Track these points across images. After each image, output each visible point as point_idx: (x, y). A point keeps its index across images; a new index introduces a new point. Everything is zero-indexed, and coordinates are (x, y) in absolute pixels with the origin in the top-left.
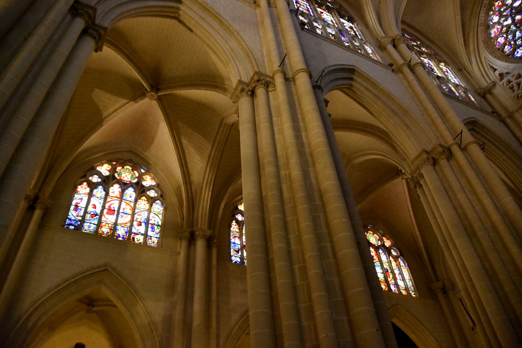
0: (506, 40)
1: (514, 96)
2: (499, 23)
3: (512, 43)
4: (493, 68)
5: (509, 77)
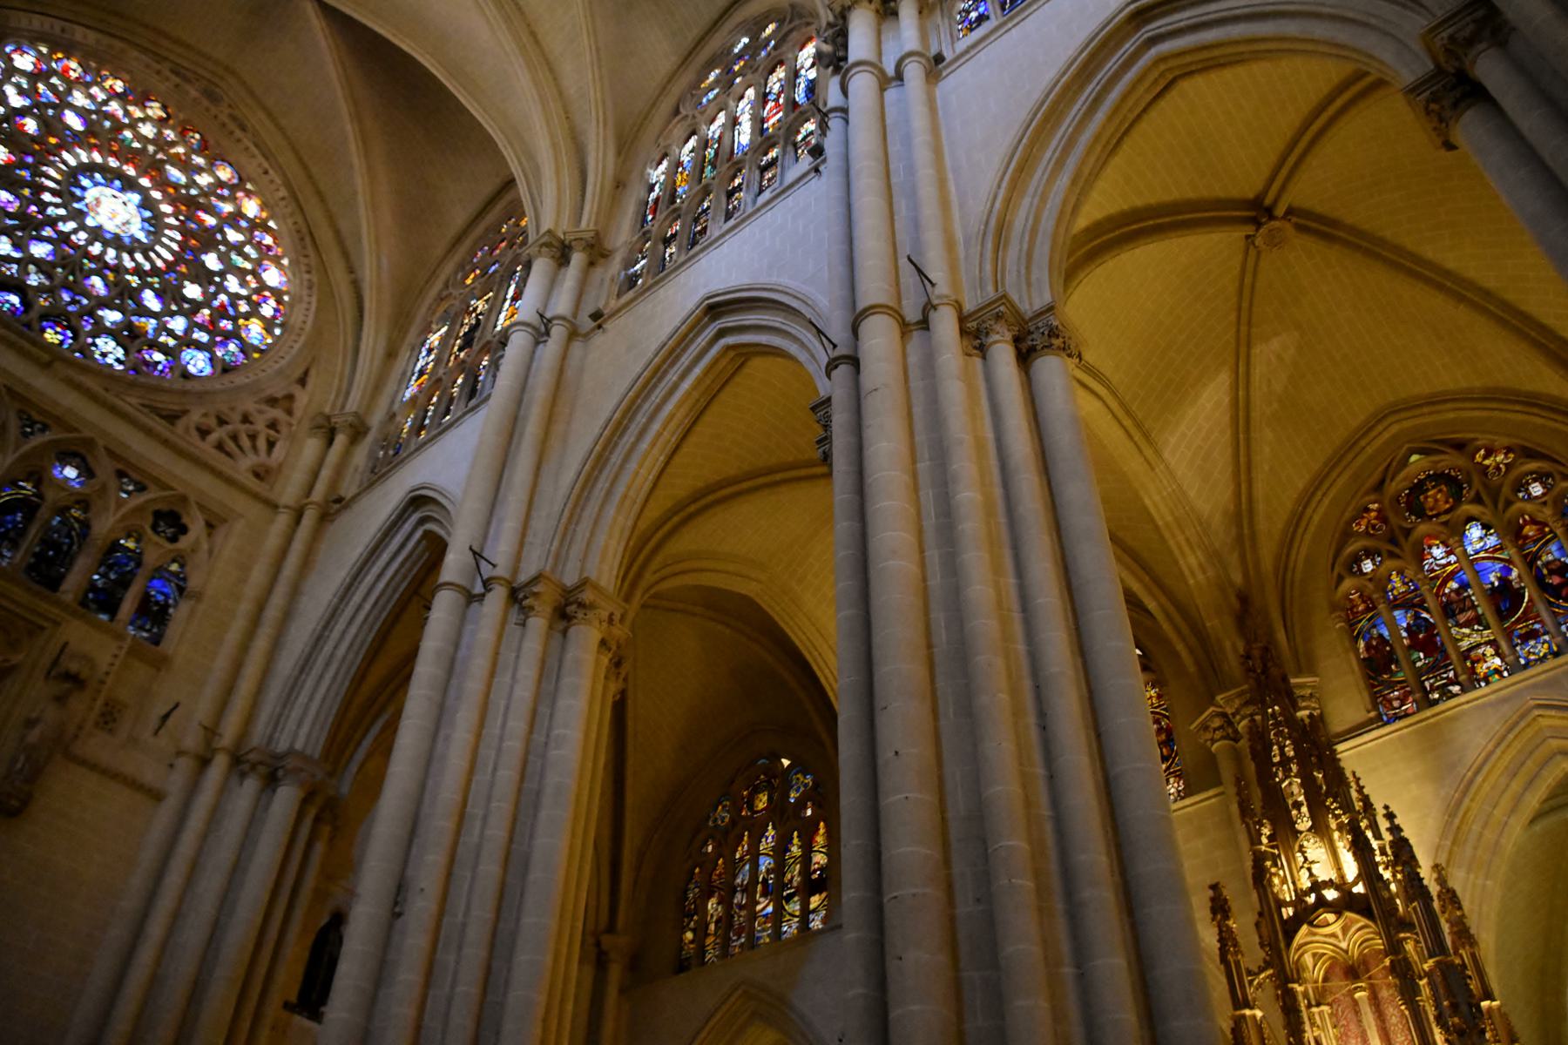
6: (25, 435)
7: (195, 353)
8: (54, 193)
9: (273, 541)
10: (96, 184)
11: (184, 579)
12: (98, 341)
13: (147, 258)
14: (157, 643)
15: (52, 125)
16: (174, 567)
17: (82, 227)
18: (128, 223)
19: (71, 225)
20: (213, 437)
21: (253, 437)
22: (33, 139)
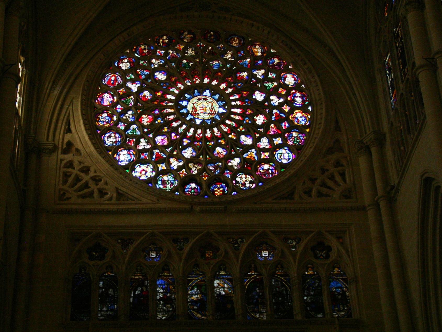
0: (113, 107)
1: (60, 190)
2: (124, 74)
3: (115, 118)
4: (69, 125)
5: (76, 159)
6: (237, 249)
7: (280, 151)
8: (175, 120)
9: (373, 228)
10: (188, 101)
11: (344, 274)
12: (238, 179)
13: (231, 120)
14: (350, 315)
15: (154, 86)
16: (336, 271)
17: (197, 127)
18: (213, 108)
19: (192, 130)
20: (314, 191)
21: (332, 178)
22: (152, 100)
